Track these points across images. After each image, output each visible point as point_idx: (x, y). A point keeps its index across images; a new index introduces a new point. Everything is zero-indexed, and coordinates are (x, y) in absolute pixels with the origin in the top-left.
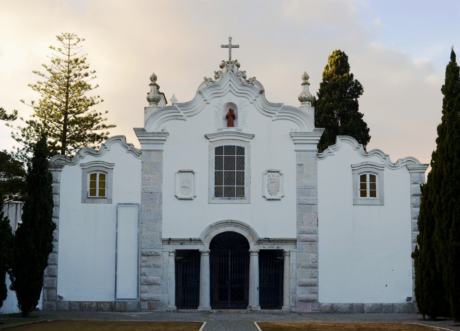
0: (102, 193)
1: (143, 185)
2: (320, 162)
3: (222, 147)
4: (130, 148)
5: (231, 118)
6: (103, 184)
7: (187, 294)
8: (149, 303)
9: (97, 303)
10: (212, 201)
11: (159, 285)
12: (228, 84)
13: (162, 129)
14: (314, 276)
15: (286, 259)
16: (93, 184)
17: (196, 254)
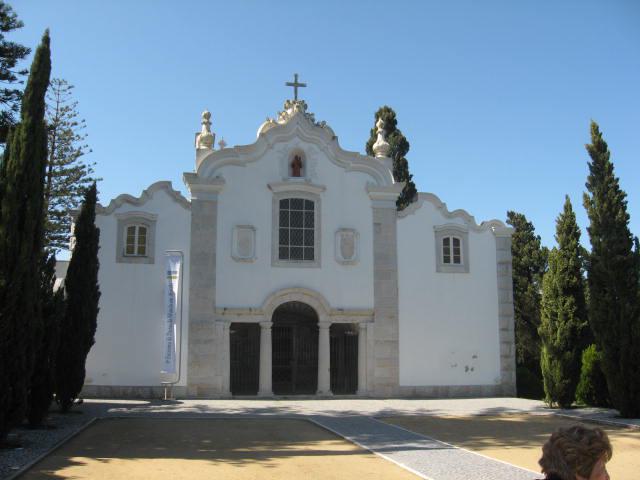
0: (142, 251)
4: (177, 197)
5: (297, 166)
6: (143, 240)
16: (130, 240)
17: (256, 328)
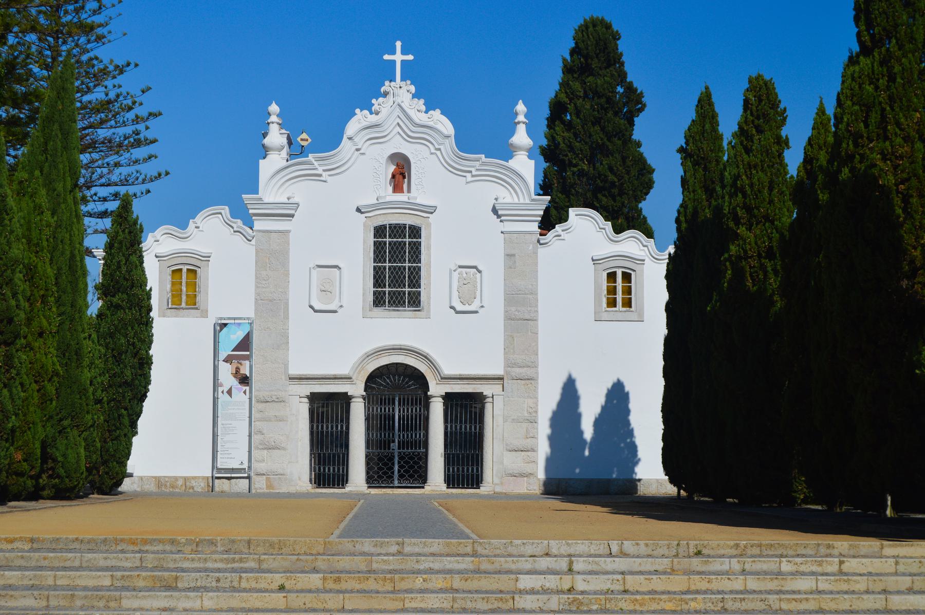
1: (257, 287)
2: (541, 251)
3: (384, 226)
7: (328, 465)
8: (268, 479)
9: (186, 479)
10: (369, 314)
11: (284, 449)
12: (395, 123)
13: (288, 196)
14: (531, 435)
15: (488, 407)
17: (344, 400)
